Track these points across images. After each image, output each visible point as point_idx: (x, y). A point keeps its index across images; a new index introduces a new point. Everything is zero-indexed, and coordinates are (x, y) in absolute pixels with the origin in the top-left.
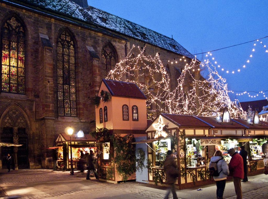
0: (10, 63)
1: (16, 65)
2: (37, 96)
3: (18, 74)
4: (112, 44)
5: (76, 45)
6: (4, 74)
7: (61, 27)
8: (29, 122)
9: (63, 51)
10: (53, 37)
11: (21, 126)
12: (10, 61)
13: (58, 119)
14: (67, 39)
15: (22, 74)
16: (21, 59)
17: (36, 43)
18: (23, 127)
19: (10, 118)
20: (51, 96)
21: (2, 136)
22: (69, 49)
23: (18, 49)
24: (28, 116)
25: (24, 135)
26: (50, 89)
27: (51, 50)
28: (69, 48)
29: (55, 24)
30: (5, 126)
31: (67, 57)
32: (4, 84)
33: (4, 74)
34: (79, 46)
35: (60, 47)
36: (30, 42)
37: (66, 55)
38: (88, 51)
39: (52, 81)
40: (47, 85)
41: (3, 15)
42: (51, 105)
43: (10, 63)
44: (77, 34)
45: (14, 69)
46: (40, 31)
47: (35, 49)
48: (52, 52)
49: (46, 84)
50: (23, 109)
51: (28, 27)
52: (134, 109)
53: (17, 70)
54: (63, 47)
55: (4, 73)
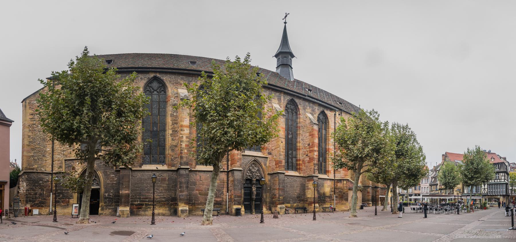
4: (325, 113)
5: (298, 112)
20: (283, 154)
38: (308, 118)
46: (273, 101)
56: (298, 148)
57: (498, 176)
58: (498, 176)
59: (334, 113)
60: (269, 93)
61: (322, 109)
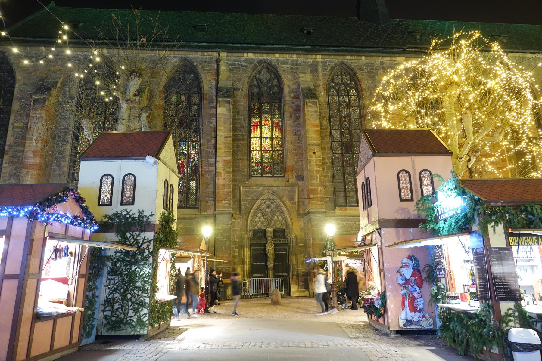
0: (261, 134)
1: (270, 135)
2: (300, 178)
3: (272, 148)
5: (360, 87)
6: (253, 150)
7: (332, 64)
8: (289, 220)
9: (339, 101)
10: (321, 83)
11: (279, 226)
12: (261, 131)
13: (335, 211)
14: (345, 81)
15: (278, 148)
16: (277, 126)
17: (296, 97)
18: (282, 227)
19: (264, 214)
21: (252, 243)
22: (348, 95)
23: (272, 113)
24: (287, 209)
25: (283, 241)
26: (317, 163)
27: (315, 103)
28: (348, 94)
29: (323, 62)
30: (256, 228)
31: (346, 109)
32: (254, 165)
33: (253, 150)
34: (364, 87)
35: (333, 95)
36: (288, 96)
37: (344, 106)
39: (320, 151)
40: (312, 159)
41: (251, 69)
42: (319, 189)
43: (261, 134)
44: (359, 69)
45: (267, 142)
47: (294, 107)
48: (317, 107)
49: (310, 157)
50: (281, 199)
51: (283, 76)
52: (424, 177)
53: (271, 142)
54: (338, 95)
55: (254, 149)
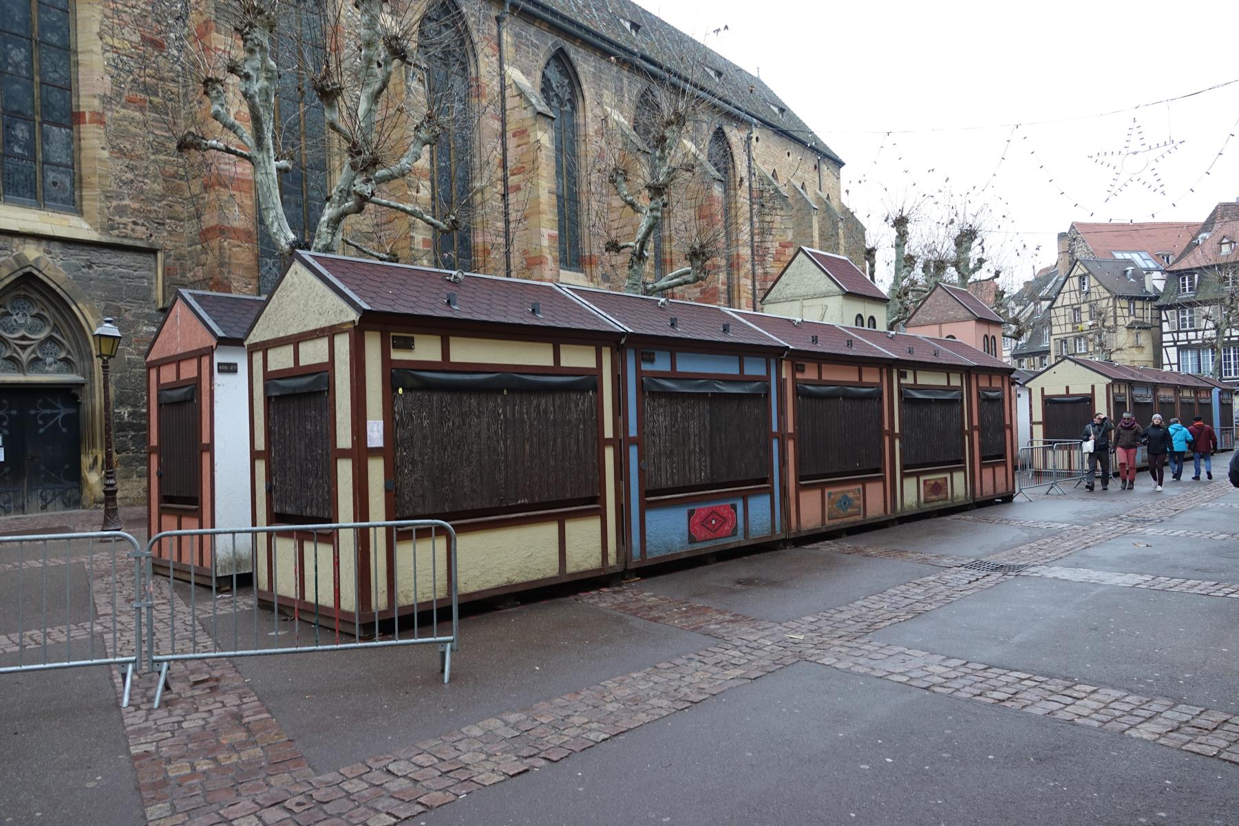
4: (723, 133)
56: (668, 257)
57: (1191, 319)
58: (1191, 319)
59: (747, 132)
60: (595, 67)
61: (717, 121)
